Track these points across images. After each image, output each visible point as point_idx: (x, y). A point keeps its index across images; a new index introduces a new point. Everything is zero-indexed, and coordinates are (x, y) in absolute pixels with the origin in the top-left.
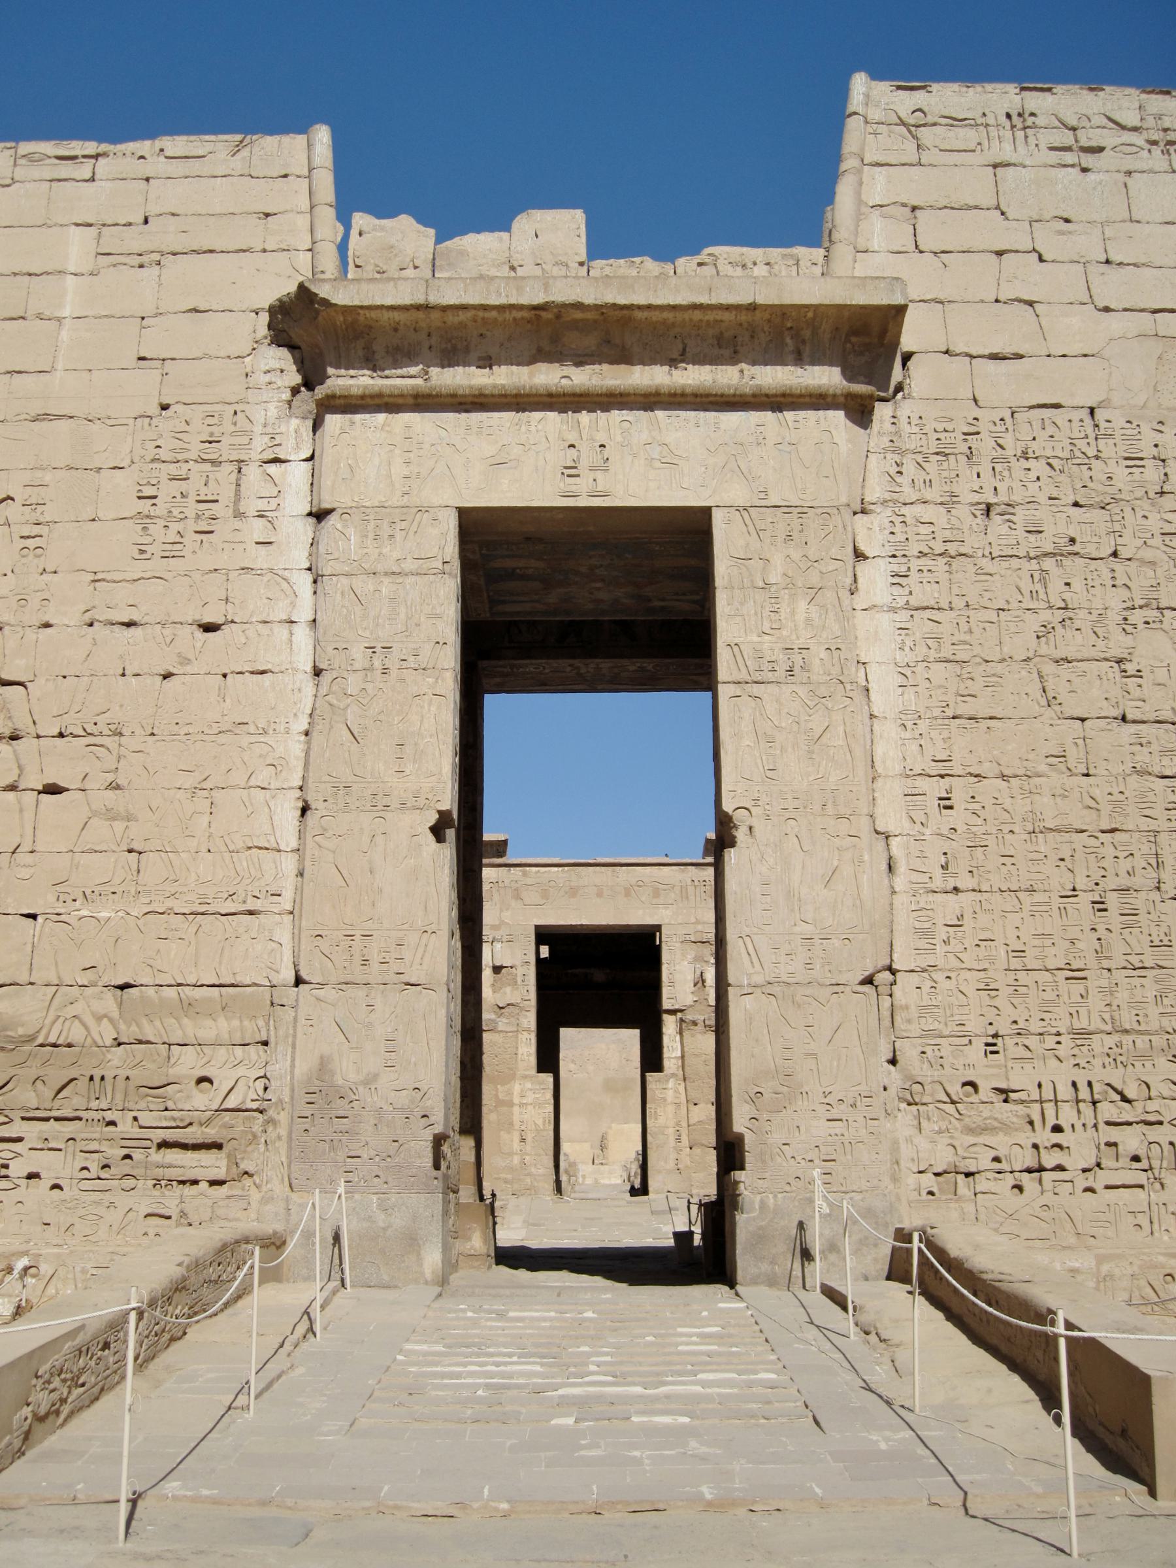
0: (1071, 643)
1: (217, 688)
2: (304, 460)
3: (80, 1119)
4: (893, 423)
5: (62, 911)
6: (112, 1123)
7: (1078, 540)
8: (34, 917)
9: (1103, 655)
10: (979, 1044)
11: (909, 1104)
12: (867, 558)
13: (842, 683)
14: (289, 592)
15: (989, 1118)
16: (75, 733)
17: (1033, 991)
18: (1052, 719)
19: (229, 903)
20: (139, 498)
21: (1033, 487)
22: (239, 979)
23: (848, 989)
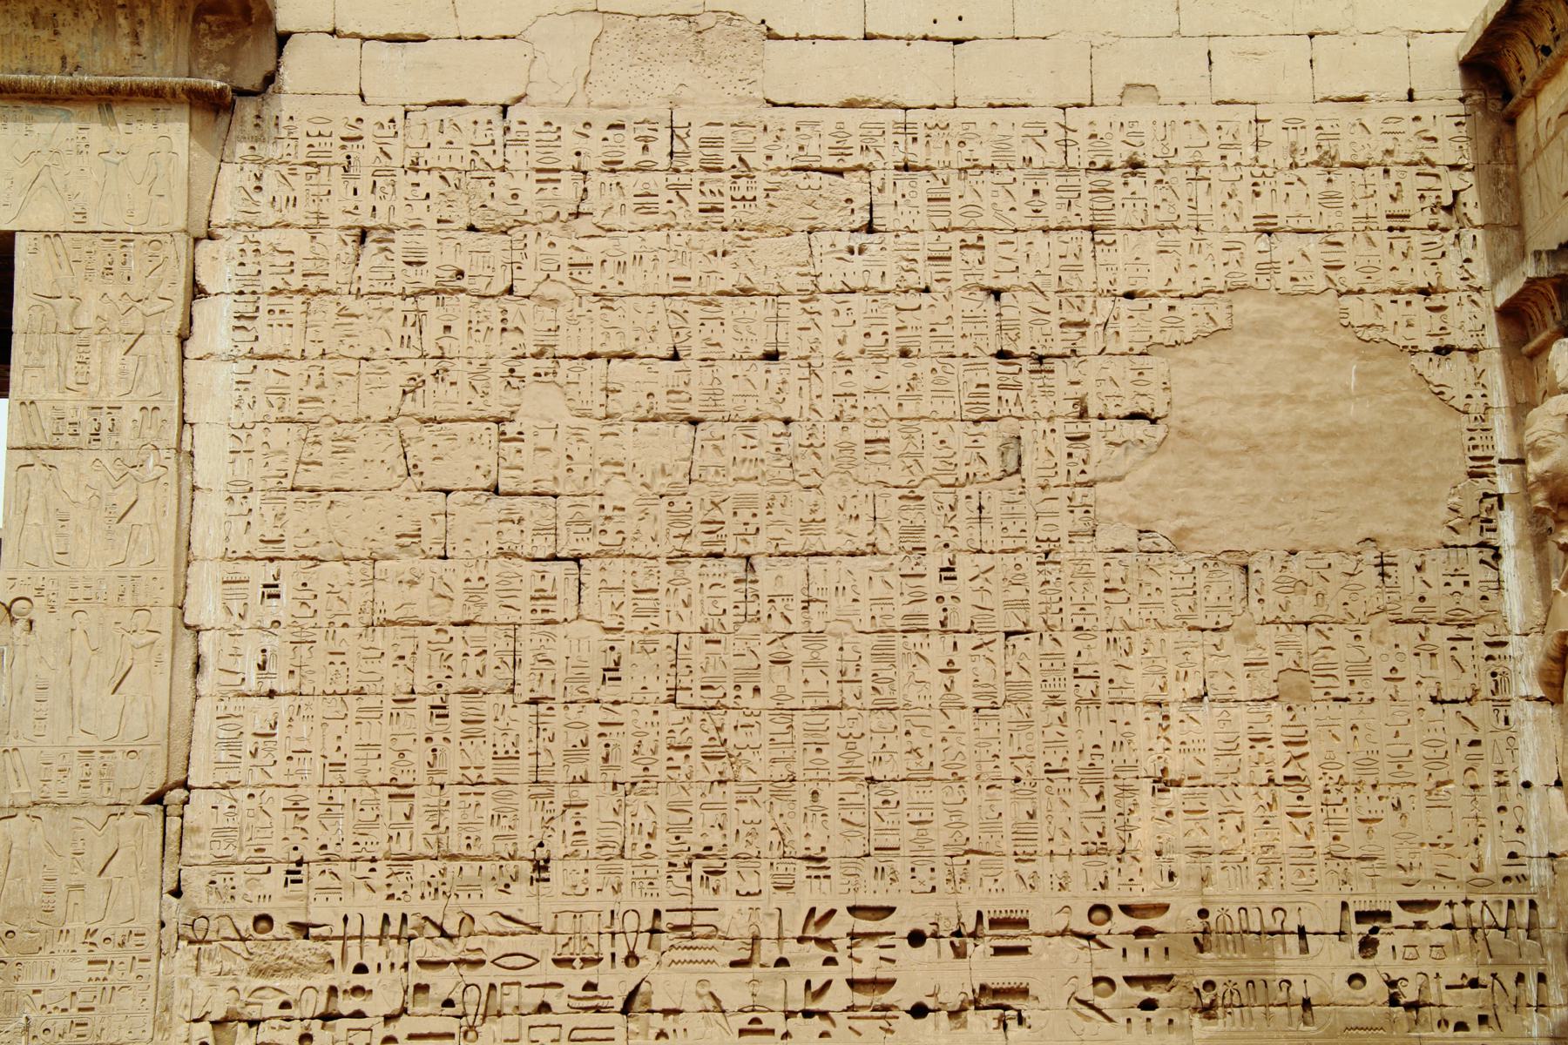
0: (438, 399)
4: (257, 125)
7: (467, 274)
9: (479, 414)
10: (279, 872)
11: (191, 942)
12: (207, 295)
13: (157, 449)
15: (283, 957)
17: (348, 811)
18: (409, 491)
21: (420, 207)
23: (130, 811)
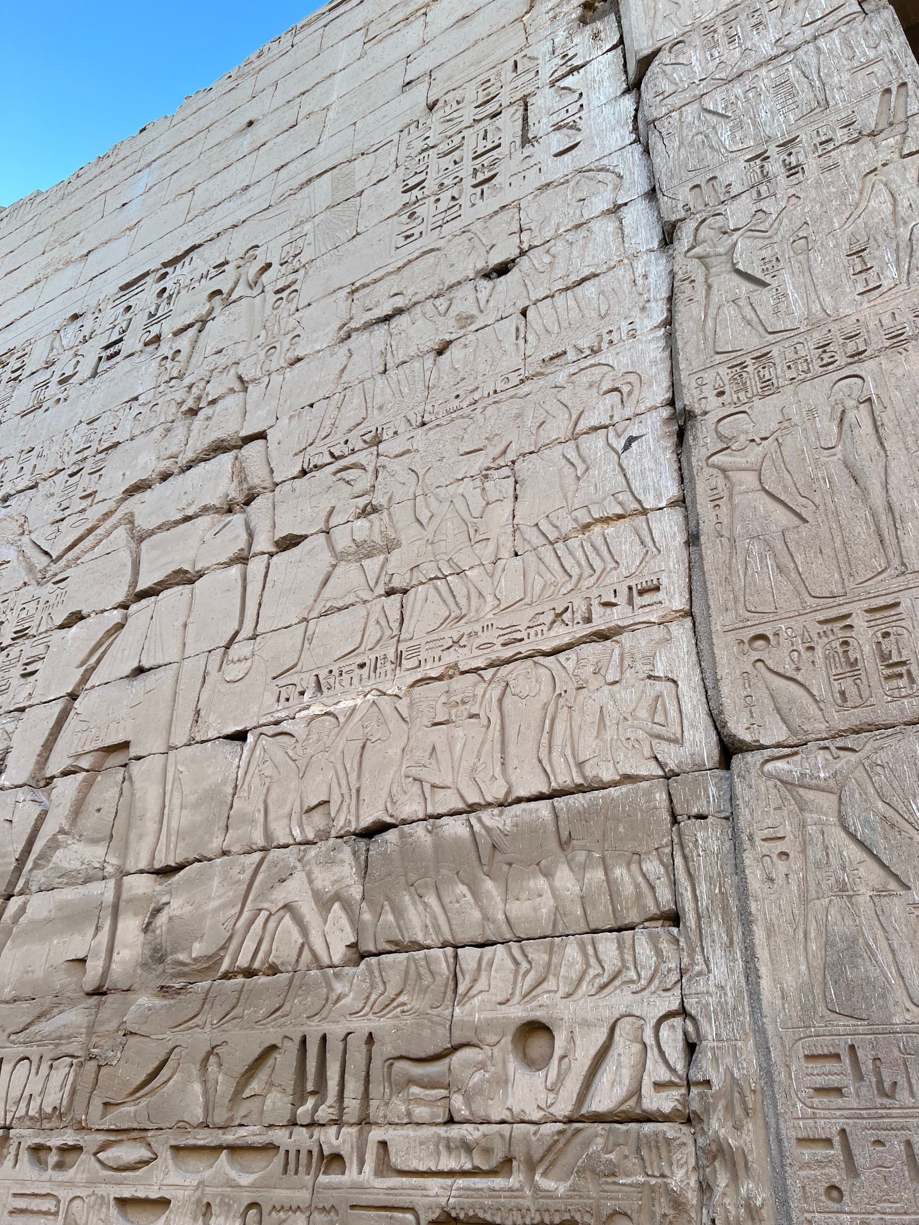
5: (283, 714)
19: (559, 629)
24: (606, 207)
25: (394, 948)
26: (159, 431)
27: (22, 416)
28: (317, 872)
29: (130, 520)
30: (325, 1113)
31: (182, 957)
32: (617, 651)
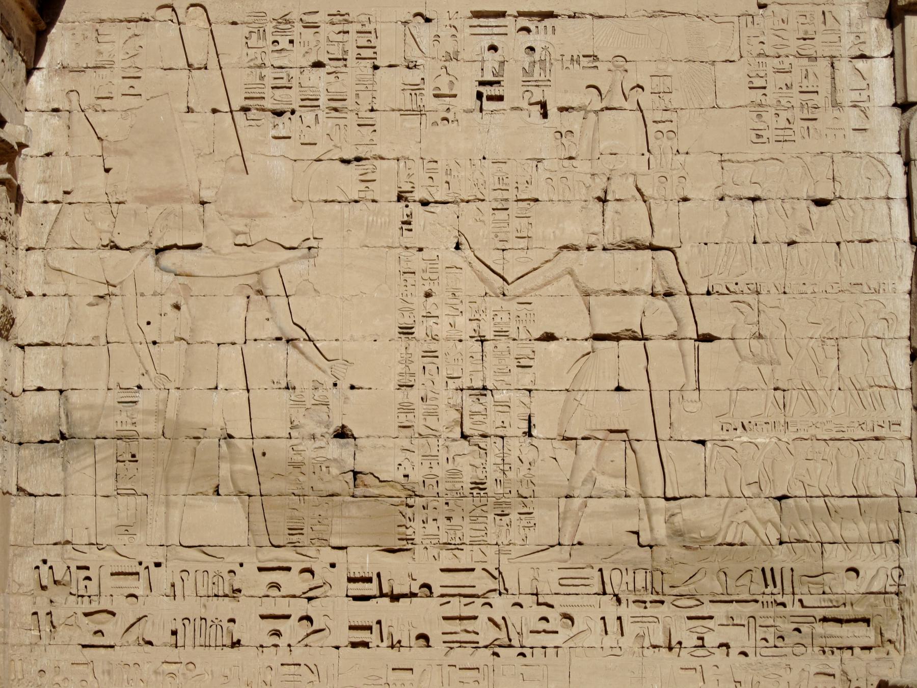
1: (833, 254)
2: (886, 57)
3: (757, 601)
5: (727, 438)
6: (784, 605)
8: (703, 442)
14: (884, 173)
16: (720, 291)
20: (750, 88)
22: (873, 491)
24: (883, 194)
25: (795, 541)
26: (577, 207)
27: (401, 115)
28: (758, 510)
29: (571, 273)
30: (775, 591)
31: (694, 535)
32: (884, 447)
